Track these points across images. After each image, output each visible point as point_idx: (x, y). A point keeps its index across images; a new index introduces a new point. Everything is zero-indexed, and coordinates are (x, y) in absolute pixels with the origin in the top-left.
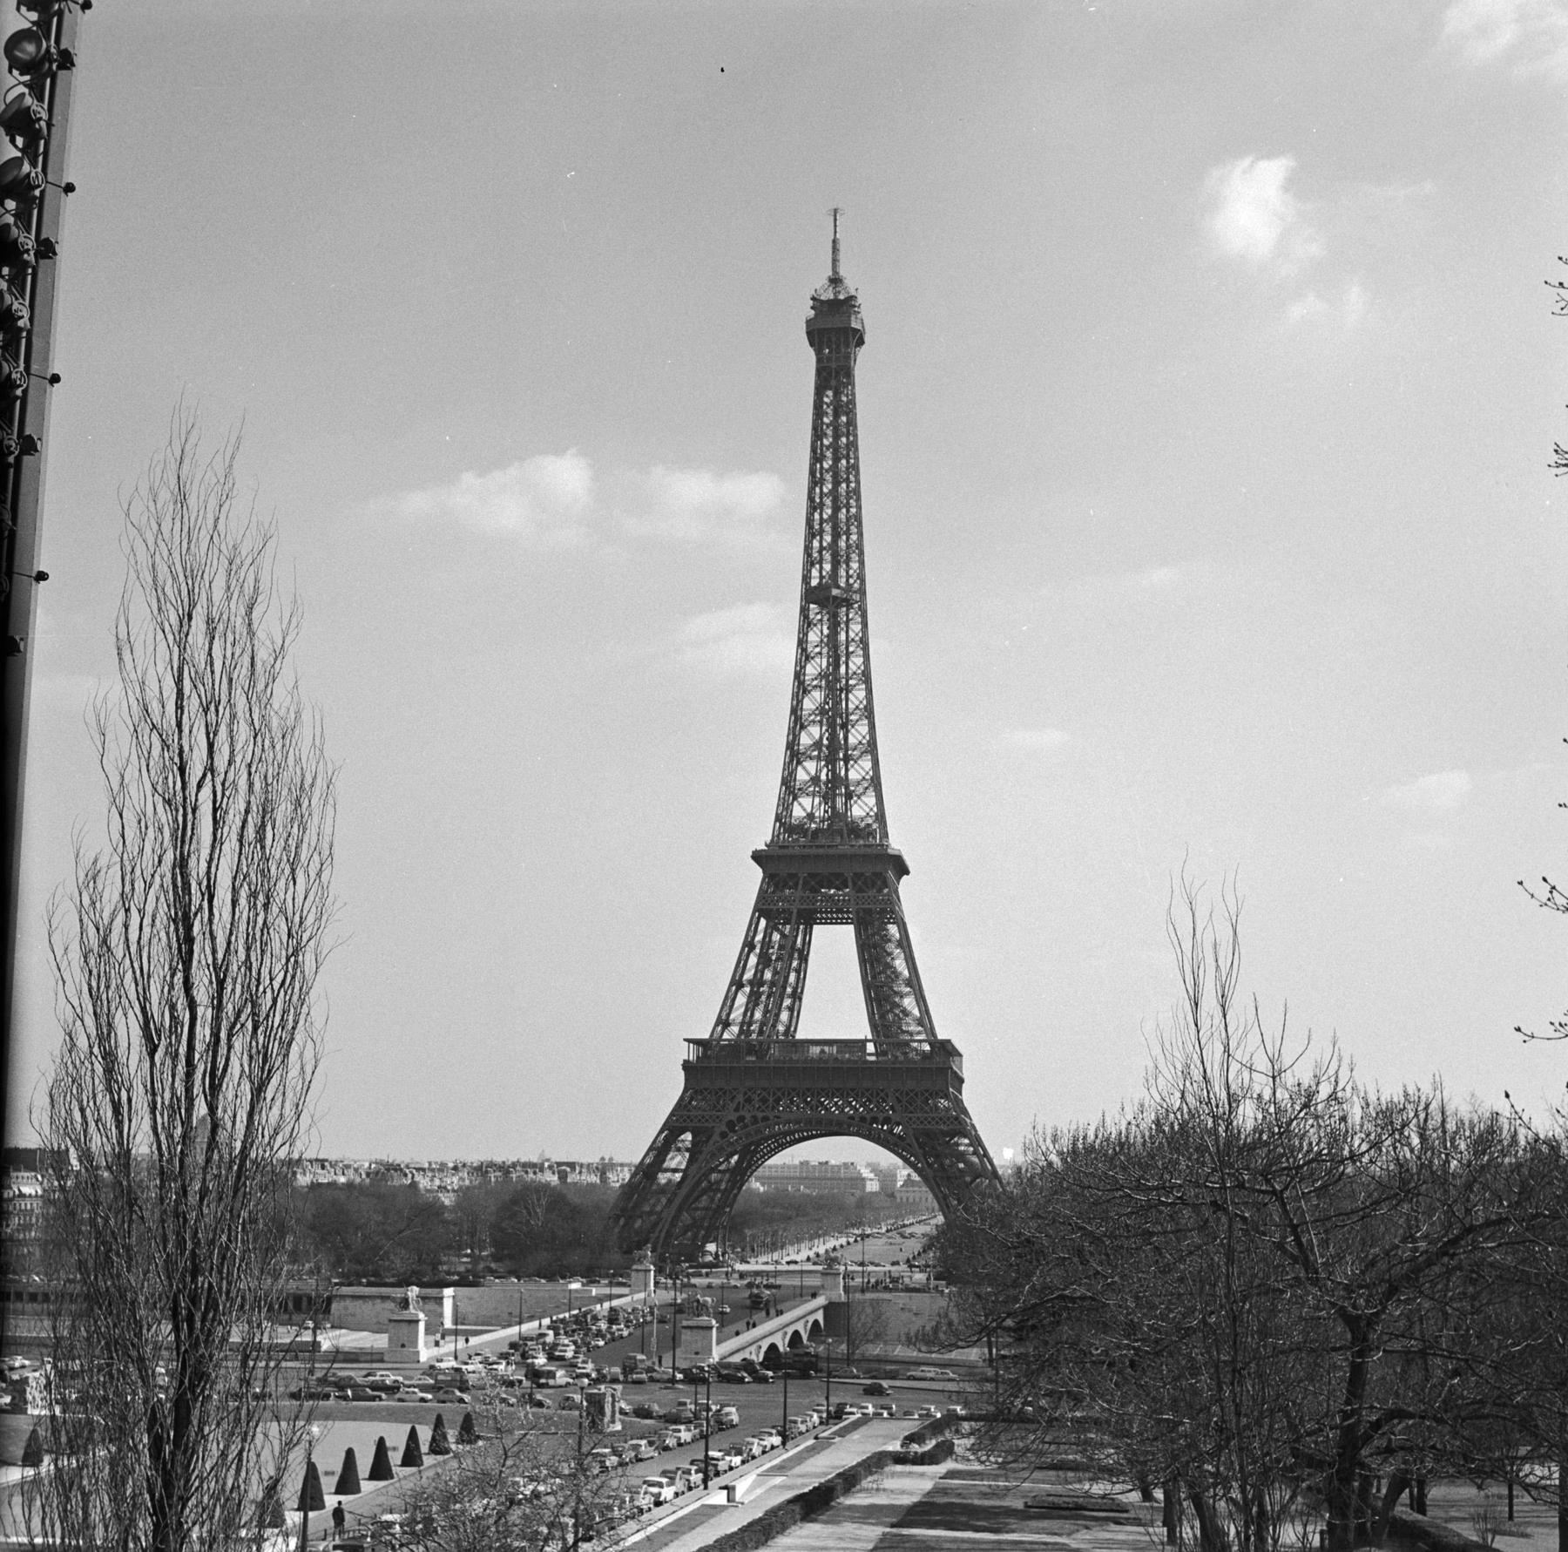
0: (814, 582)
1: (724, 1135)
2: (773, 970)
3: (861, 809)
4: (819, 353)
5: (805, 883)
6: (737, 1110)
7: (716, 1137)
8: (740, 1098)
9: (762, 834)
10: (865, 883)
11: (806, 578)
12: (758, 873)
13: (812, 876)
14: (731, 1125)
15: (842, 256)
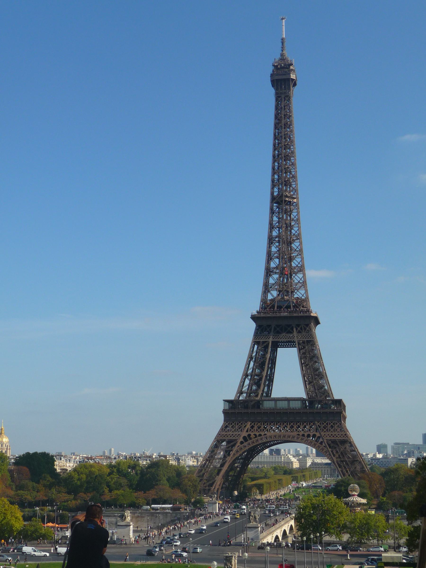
0: (276, 194)
1: (242, 443)
2: (262, 368)
3: (299, 294)
4: (276, 89)
5: (275, 329)
6: (247, 431)
7: (238, 444)
8: (248, 426)
9: (255, 307)
10: (301, 329)
11: (272, 193)
12: (253, 325)
13: (278, 326)
14: (244, 438)
15: (285, 44)
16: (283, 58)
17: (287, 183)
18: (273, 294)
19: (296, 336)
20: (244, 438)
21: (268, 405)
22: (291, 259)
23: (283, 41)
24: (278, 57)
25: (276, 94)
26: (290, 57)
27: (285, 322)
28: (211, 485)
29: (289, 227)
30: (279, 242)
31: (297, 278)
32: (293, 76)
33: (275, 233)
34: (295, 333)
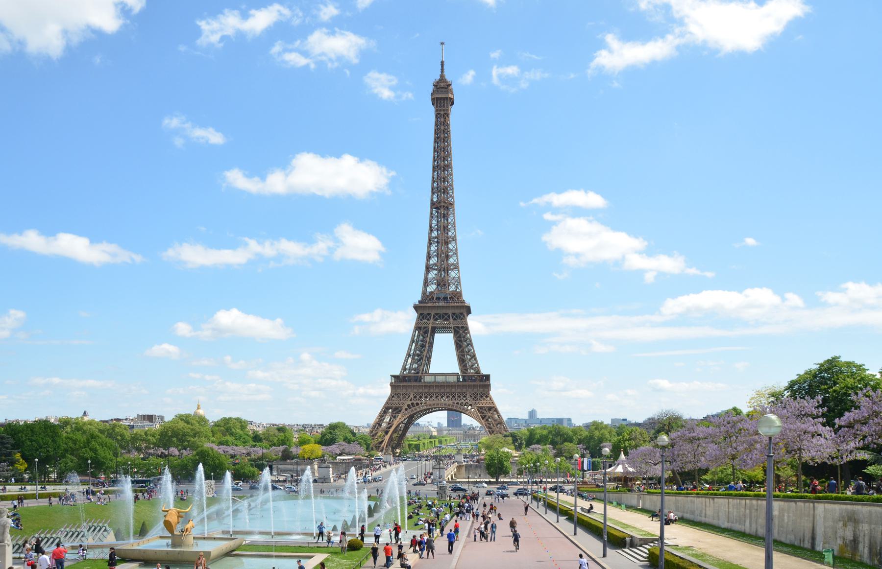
1: (406, 409)
7: (403, 410)
8: (412, 396)
9: (417, 297)
11: (432, 200)
13: (437, 314)
14: (408, 406)
16: (442, 78)
17: (445, 191)
18: (432, 288)
19: (451, 323)
20: (408, 406)
21: (427, 379)
22: (447, 257)
23: (442, 63)
24: (438, 78)
25: (437, 111)
26: (448, 77)
27: (443, 310)
28: (381, 443)
29: (446, 229)
30: (438, 242)
31: (452, 274)
32: (450, 96)
33: (435, 234)
34: (451, 320)
